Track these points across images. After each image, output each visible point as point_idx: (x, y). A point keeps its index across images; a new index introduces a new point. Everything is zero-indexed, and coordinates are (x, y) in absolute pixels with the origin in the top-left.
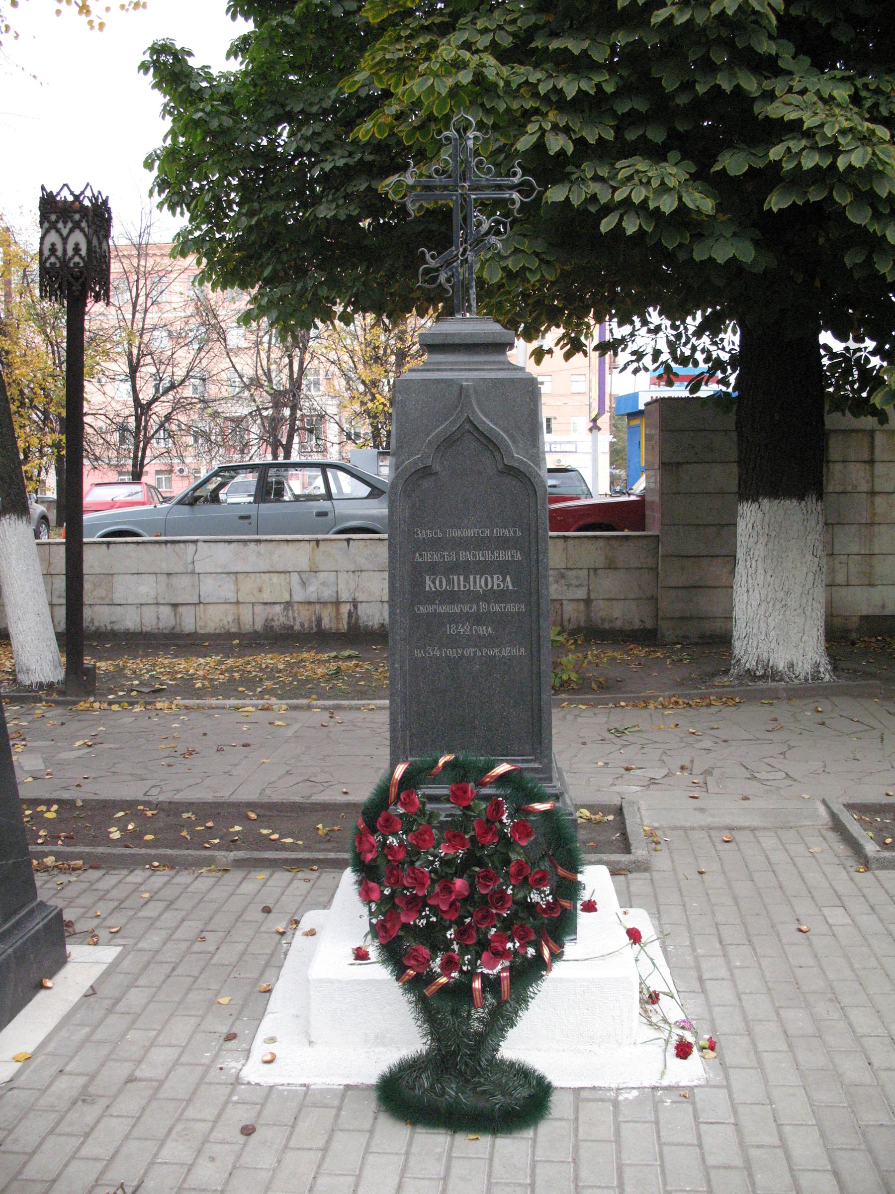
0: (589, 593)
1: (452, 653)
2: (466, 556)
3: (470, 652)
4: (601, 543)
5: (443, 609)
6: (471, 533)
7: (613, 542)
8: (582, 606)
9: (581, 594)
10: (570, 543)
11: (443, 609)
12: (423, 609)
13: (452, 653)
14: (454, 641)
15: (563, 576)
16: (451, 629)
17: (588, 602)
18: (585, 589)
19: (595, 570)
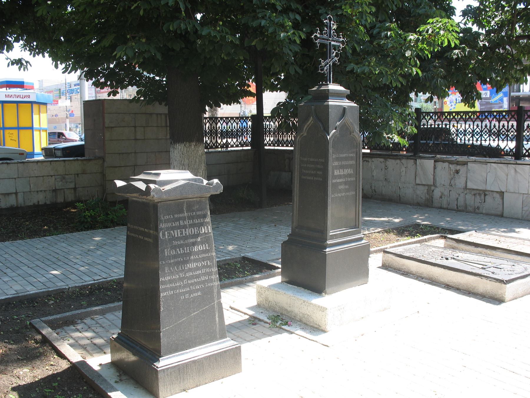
0: (75, 185)
1: (340, 195)
2: (344, 163)
3: (343, 194)
4: (80, 162)
5: (338, 181)
6: (344, 155)
7: (85, 162)
8: (73, 191)
9: (72, 185)
10: (67, 162)
11: (338, 181)
12: (334, 181)
13: (340, 195)
14: (340, 191)
15: (64, 178)
16: (340, 187)
17: (75, 189)
18: (74, 183)
19: (78, 174)
